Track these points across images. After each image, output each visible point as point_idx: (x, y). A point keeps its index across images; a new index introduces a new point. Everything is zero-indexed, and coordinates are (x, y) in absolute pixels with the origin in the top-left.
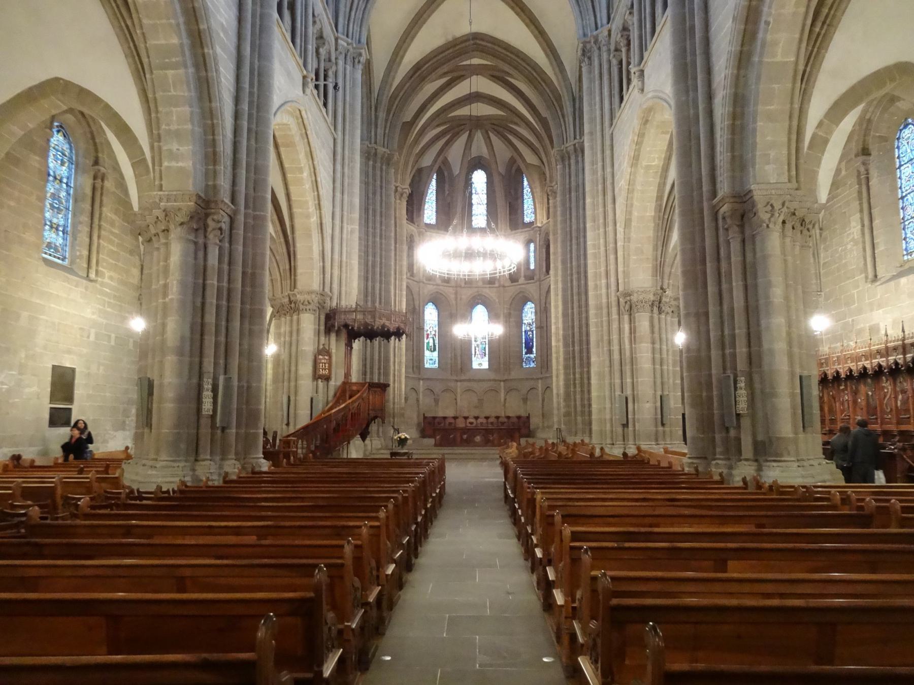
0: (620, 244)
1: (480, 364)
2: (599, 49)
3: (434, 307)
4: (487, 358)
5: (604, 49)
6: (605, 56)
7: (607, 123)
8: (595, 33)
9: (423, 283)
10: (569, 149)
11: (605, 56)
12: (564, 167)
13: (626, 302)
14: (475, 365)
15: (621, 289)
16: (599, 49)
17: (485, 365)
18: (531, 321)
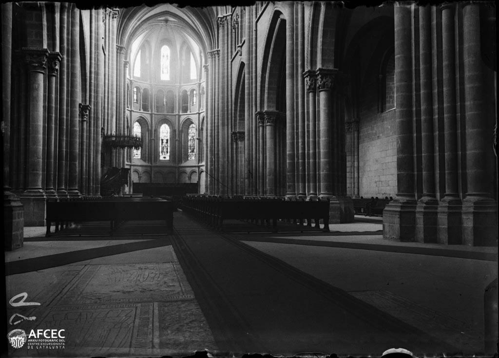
0: (233, 112)
1: (165, 158)
2: (227, 23)
3: (139, 125)
4: (169, 154)
5: (229, 24)
6: (230, 27)
7: (230, 57)
8: (225, 15)
9: (133, 111)
10: (215, 53)
11: (230, 27)
12: (212, 61)
13: (234, 137)
14: (161, 158)
15: (233, 131)
16: (227, 23)
17: (168, 158)
18: (193, 135)
